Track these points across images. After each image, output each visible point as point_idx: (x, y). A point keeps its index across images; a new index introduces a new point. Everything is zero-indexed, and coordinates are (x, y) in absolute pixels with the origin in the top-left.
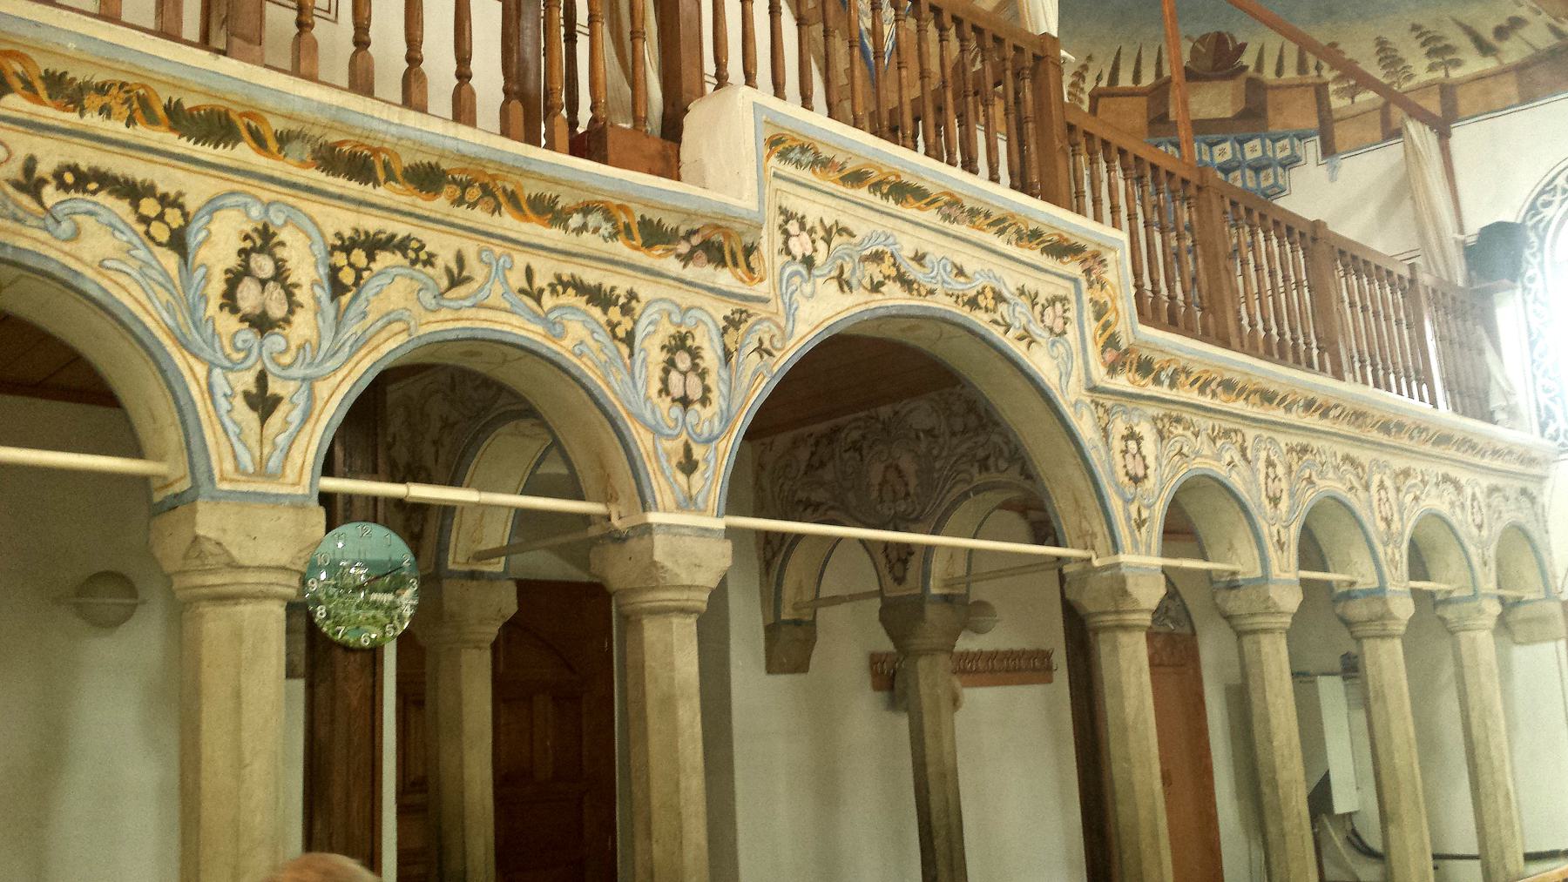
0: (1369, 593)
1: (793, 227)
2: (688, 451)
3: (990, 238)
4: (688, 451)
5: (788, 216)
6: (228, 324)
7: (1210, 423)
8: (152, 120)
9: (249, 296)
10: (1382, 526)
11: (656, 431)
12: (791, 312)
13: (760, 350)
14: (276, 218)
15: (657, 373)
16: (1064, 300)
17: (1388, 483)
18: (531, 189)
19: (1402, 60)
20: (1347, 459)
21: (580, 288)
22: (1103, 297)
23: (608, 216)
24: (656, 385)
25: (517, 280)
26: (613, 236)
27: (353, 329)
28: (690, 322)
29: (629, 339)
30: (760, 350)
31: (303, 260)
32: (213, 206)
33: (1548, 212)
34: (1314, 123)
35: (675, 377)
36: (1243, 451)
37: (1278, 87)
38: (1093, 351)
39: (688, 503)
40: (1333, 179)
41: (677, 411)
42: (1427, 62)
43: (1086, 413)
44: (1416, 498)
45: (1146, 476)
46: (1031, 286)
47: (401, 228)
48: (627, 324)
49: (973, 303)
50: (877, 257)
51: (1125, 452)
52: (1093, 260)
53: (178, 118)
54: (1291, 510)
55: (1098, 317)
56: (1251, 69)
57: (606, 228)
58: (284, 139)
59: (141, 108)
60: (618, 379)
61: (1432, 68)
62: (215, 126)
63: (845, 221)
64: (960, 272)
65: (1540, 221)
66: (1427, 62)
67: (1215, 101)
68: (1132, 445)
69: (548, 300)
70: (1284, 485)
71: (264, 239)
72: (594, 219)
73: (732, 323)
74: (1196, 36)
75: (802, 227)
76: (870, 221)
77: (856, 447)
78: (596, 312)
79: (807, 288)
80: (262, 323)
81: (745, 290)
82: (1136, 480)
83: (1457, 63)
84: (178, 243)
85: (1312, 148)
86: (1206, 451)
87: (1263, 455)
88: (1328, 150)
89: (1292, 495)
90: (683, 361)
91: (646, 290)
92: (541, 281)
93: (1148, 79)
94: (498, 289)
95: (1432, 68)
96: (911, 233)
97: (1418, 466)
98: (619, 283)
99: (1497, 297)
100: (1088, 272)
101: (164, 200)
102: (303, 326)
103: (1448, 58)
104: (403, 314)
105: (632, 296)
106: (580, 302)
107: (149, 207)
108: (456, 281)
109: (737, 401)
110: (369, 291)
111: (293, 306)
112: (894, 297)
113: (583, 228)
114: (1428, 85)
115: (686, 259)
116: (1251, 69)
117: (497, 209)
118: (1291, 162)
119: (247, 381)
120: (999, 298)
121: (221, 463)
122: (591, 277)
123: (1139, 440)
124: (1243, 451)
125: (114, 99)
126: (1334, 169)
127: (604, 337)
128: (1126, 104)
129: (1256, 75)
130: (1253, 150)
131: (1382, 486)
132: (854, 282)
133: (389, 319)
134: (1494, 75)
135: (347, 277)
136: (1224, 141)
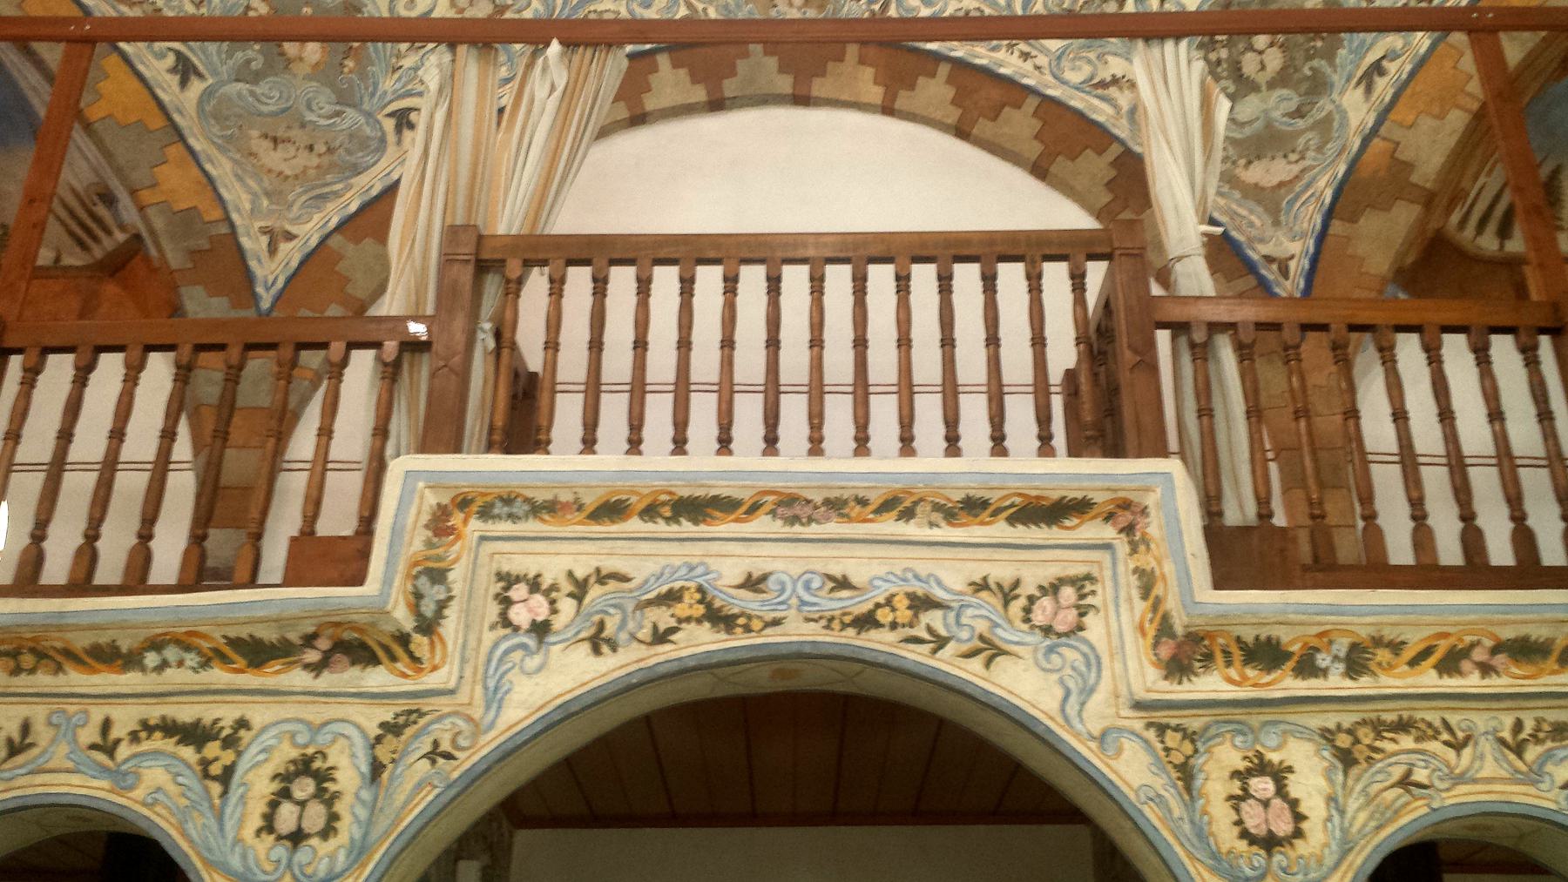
3: (889, 526)
5: (508, 580)
7: (1508, 720)
12: (495, 697)
13: (435, 754)
21: (169, 728)
22: (1146, 561)
24: (256, 821)
25: (90, 735)
26: (205, 664)
28: (323, 739)
29: (229, 771)
30: (435, 754)
41: (281, 851)
43: (1131, 747)
45: (1298, 834)
46: (1001, 571)
48: (228, 757)
49: (866, 621)
52: (1126, 513)
55: (1146, 592)
57: (191, 659)
63: (609, 565)
64: (843, 583)
68: (1263, 786)
69: (123, 751)
72: (171, 653)
73: (392, 729)
78: (188, 753)
79: (533, 662)
81: (408, 686)
82: (1270, 843)
91: (259, 714)
94: (63, 749)
98: (226, 714)
100: (1129, 529)
105: (242, 724)
106: (169, 745)
109: (383, 823)
112: (700, 641)
113: (164, 665)
115: (316, 669)
117: (59, 669)
120: (922, 603)
122: (185, 713)
123: (1279, 775)
127: (191, 780)
132: (623, 636)
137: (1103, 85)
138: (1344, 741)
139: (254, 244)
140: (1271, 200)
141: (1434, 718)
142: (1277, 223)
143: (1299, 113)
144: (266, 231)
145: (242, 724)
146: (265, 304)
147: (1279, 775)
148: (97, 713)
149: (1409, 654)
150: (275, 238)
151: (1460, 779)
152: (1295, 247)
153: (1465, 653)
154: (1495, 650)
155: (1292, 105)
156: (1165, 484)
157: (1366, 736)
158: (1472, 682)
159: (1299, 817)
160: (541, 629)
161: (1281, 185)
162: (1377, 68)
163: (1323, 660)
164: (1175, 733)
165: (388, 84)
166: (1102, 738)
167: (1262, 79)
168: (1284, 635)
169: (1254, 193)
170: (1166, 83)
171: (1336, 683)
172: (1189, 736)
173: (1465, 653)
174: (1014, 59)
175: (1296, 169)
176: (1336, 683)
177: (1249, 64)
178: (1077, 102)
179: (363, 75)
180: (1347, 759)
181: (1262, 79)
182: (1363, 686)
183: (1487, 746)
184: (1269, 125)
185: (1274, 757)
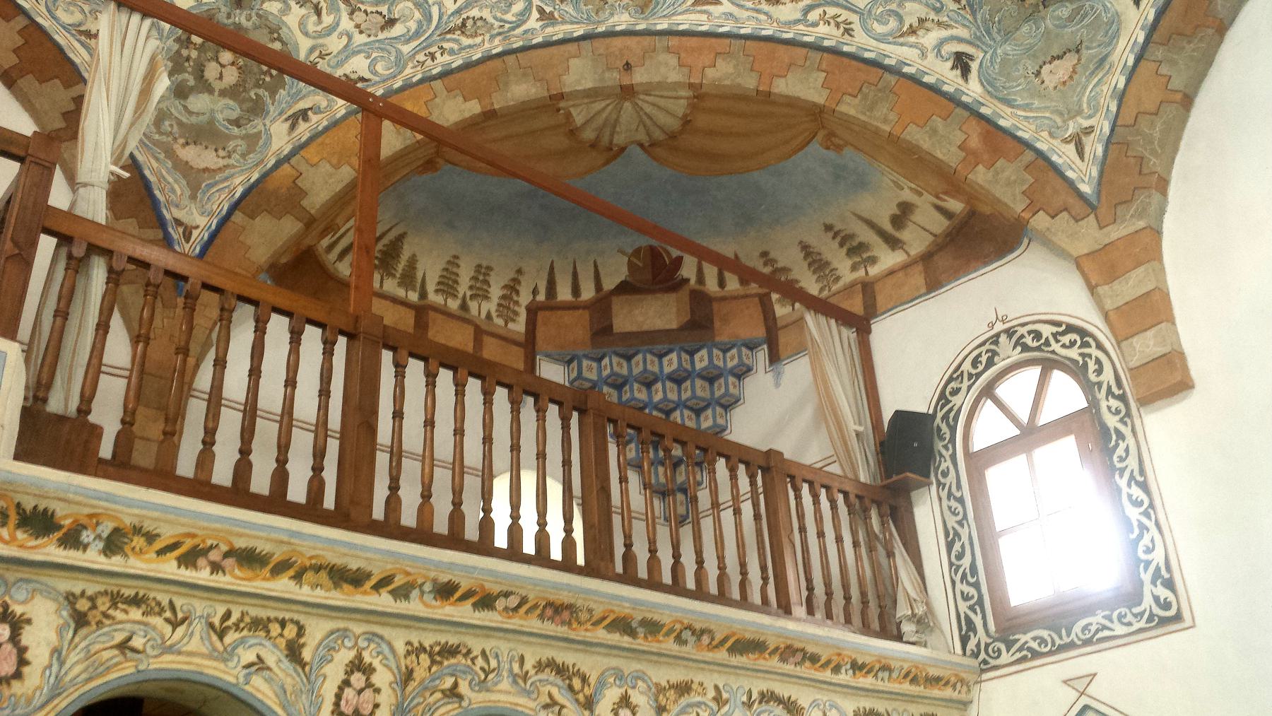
7: (221, 610)
17: (637, 698)
19: (828, 263)
20: (551, 664)
33: (957, 400)
34: (760, 332)
36: (293, 652)
37: (723, 299)
40: (777, 385)
42: (849, 263)
56: (693, 281)
61: (854, 268)
65: (951, 409)
66: (849, 263)
67: (658, 313)
74: (630, 251)
83: (873, 260)
85: (762, 355)
87: (345, 656)
88: (774, 358)
93: (588, 293)
95: (854, 268)
97: (711, 680)
99: (915, 495)
103: (865, 256)
114: (852, 285)
116: (693, 281)
118: (742, 373)
124: (293, 652)
126: (778, 375)
128: (568, 317)
129: (698, 287)
130: (701, 360)
134: (905, 267)
136: (671, 351)
138: (83, 605)
140: (195, 179)
141: (164, 599)
142: (193, 197)
143: (237, 123)
149: (159, 545)
151: (170, 650)
152: (202, 221)
153: (205, 552)
154: (227, 555)
155: (234, 115)
157: (103, 604)
159: (22, 662)
161: (206, 170)
162: (304, 114)
163: (86, 536)
168: (60, 510)
169: (184, 168)
170: (123, 45)
171: (93, 557)
173: (205, 552)
175: (221, 163)
176: (93, 557)
177: (211, 71)
180: (80, 620)
181: (218, 86)
182: (115, 563)
183: (198, 627)
184: (212, 121)
185: (18, 609)
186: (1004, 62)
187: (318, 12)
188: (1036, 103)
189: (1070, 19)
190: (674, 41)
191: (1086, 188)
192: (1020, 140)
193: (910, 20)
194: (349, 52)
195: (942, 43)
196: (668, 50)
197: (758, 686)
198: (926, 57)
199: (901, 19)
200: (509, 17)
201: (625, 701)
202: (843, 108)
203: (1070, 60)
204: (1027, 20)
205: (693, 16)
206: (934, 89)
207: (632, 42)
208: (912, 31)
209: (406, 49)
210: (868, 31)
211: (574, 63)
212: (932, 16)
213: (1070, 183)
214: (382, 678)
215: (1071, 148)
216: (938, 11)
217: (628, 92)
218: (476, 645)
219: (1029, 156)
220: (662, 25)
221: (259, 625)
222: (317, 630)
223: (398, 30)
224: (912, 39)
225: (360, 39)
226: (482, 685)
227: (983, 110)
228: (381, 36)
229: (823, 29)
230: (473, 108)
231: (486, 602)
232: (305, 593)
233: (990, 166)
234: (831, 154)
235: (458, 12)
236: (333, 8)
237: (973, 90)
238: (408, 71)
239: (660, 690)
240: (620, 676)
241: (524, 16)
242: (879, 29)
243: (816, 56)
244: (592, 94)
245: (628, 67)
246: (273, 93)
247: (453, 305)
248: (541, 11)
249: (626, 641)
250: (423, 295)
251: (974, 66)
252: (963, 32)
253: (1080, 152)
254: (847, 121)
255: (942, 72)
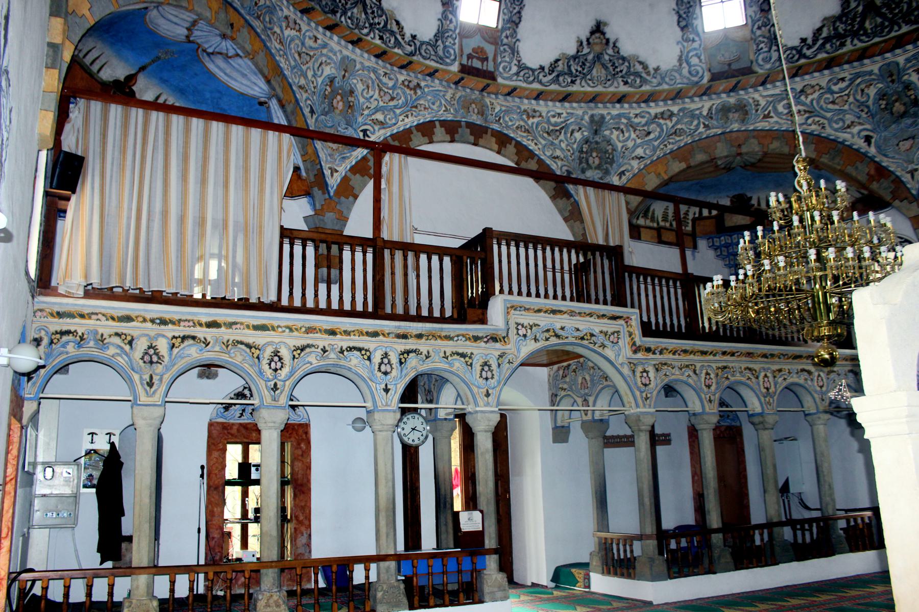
0: (759, 414)
1: (520, 327)
2: (487, 391)
3: (588, 318)
4: (487, 391)
5: (518, 324)
6: (379, 374)
8: (363, 335)
9: (383, 368)
10: (764, 391)
11: (479, 387)
12: (519, 350)
13: (509, 362)
14: (388, 350)
15: (479, 372)
16: (618, 332)
17: (769, 375)
18: (443, 334)
21: (458, 354)
22: (631, 330)
23: (463, 336)
25: (442, 354)
27: (405, 372)
29: (471, 364)
30: (509, 362)
31: (394, 359)
32: (375, 350)
35: (484, 373)
36: (695, 372)
38: (628, 348)
39: (488, 404)
41: (484, 381)
44: (785, 379)
46: (605, 329)
47: (414, 348)
49: (582, 338)
50: (548, 331)
51: (641, 377)
53: (368, 334)
54: (717, 389)
58: (388, 334)
59: (361, 333)
60: (468, 375)
62: (375, 334)
63: (536, 322)
64: (578, 330)
68: (645, 374)
69: (450, 358)
70: (714, 381)
71: (386, 355)
73: (501, 356)
75: (523, 326)
76: (544, 321)
77: (574, 371)
78: (462, 359)
80: (386, 373)
82: (646, 385)
84: (369, 359)
86: (677, 373)
87: (704, 372)
89: (717, 383)
90: (486, 368)
92: (448, 354)
96: (558, 322)
97: (787, 367)
101: (366, 350)
102: (394, 373)
104: (414, 366)
105: (472, 354)
106: (458, 357)
107: (363, 352)
108: (427, 357)
110: (408, 363)
111: (392, 368)
112: (554, 340)
115: (486, 342)
119: (383, 386)
120: (592, 335)
121: (379, 404)
122: (460, 351)
123: (647, 372)
124: (695, 372)
125: (356, 333)
127: (464, 365)
128: (708, 222)
131: (766, 376)
133: (412, 368)
135: (403, 360)
137: (554, 158)
139: (327, 173)
144: (330, 168)
145: (472, 354)
146: (332, 194)
147: (647, 372)
148: (443, 350)
150: (333, 171)
155: (600, 176)
156: (633, 314)
158: (677, 357)
160: (525, 336)
162: (623, 173)
164: (633, 365)
165: (360, 119)
166: (621, 365)
167: (594, 166)
172: (635, 365)
174: (533, 144)
178: (548, 162)
179: (353, 116)
180: (657, 370)
181: (594, 166)
186: (885, 140)
187: (623, 132)
188: (897, 156)
189: (911, 125)
190: (756, 133)
191: (914, 192)
192: (890, 171)
193: (848, 123)
194: (636, 146)
195: (861, 131)
196: (754, 137)
197: (800, 367)
198: (853, 138)
199: (844, 122)
200: (692, 127)
201: (766, 376)
202: (822, 160)
203: (910, 142)
204: (894, 122)
205: (763, 124)
206: (857, 150)
207: (740, 134)
208: (849, 127)
209: (656, 143)
210: (831, 127)
211: (719, 144)
212: (857, 120)
213: (908, 189)
214: (712, 376)
215: (909, 176)
216: (859, 118)
217: (740, 154)
218: (730, 365)
219: (893, 177)
220: (751, 128)
221: (687, 366)
222: (698, 365)
223: (652, 136)
224: (848, 130)
225: (639, 141)
226: (733, 375)
227: (877, 159)
228: (646, 139)
229: (813, 127)
230: (683, 166)
231: (733, 354)
232: (696, 358)
233: (878, 181)
234: (816, 171)
235: (673, 127)
236: (628, 131)
237: (872, 150)
238: (658, 152)
239: (774, 372)
240: (764, 369)
241: (698, 126)
242: (836, 126)
243: (811, 137)
244: (726, 157)
245: (739, 146)
246: (611, 165)
247: (668, 225)
248: (704, 124)
249: (765, 360)
250: (658, 224)
251: (873, 140)
252: (868, 126)
253: (913, 177)
254: (824, 164)
255: (860, 144)
